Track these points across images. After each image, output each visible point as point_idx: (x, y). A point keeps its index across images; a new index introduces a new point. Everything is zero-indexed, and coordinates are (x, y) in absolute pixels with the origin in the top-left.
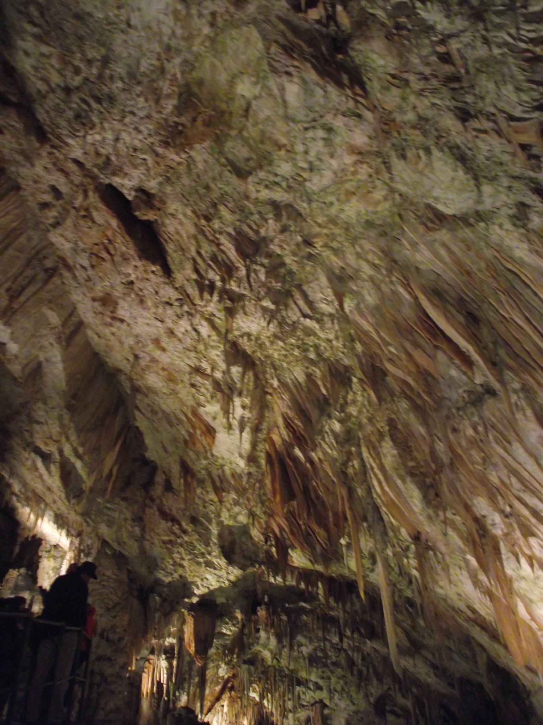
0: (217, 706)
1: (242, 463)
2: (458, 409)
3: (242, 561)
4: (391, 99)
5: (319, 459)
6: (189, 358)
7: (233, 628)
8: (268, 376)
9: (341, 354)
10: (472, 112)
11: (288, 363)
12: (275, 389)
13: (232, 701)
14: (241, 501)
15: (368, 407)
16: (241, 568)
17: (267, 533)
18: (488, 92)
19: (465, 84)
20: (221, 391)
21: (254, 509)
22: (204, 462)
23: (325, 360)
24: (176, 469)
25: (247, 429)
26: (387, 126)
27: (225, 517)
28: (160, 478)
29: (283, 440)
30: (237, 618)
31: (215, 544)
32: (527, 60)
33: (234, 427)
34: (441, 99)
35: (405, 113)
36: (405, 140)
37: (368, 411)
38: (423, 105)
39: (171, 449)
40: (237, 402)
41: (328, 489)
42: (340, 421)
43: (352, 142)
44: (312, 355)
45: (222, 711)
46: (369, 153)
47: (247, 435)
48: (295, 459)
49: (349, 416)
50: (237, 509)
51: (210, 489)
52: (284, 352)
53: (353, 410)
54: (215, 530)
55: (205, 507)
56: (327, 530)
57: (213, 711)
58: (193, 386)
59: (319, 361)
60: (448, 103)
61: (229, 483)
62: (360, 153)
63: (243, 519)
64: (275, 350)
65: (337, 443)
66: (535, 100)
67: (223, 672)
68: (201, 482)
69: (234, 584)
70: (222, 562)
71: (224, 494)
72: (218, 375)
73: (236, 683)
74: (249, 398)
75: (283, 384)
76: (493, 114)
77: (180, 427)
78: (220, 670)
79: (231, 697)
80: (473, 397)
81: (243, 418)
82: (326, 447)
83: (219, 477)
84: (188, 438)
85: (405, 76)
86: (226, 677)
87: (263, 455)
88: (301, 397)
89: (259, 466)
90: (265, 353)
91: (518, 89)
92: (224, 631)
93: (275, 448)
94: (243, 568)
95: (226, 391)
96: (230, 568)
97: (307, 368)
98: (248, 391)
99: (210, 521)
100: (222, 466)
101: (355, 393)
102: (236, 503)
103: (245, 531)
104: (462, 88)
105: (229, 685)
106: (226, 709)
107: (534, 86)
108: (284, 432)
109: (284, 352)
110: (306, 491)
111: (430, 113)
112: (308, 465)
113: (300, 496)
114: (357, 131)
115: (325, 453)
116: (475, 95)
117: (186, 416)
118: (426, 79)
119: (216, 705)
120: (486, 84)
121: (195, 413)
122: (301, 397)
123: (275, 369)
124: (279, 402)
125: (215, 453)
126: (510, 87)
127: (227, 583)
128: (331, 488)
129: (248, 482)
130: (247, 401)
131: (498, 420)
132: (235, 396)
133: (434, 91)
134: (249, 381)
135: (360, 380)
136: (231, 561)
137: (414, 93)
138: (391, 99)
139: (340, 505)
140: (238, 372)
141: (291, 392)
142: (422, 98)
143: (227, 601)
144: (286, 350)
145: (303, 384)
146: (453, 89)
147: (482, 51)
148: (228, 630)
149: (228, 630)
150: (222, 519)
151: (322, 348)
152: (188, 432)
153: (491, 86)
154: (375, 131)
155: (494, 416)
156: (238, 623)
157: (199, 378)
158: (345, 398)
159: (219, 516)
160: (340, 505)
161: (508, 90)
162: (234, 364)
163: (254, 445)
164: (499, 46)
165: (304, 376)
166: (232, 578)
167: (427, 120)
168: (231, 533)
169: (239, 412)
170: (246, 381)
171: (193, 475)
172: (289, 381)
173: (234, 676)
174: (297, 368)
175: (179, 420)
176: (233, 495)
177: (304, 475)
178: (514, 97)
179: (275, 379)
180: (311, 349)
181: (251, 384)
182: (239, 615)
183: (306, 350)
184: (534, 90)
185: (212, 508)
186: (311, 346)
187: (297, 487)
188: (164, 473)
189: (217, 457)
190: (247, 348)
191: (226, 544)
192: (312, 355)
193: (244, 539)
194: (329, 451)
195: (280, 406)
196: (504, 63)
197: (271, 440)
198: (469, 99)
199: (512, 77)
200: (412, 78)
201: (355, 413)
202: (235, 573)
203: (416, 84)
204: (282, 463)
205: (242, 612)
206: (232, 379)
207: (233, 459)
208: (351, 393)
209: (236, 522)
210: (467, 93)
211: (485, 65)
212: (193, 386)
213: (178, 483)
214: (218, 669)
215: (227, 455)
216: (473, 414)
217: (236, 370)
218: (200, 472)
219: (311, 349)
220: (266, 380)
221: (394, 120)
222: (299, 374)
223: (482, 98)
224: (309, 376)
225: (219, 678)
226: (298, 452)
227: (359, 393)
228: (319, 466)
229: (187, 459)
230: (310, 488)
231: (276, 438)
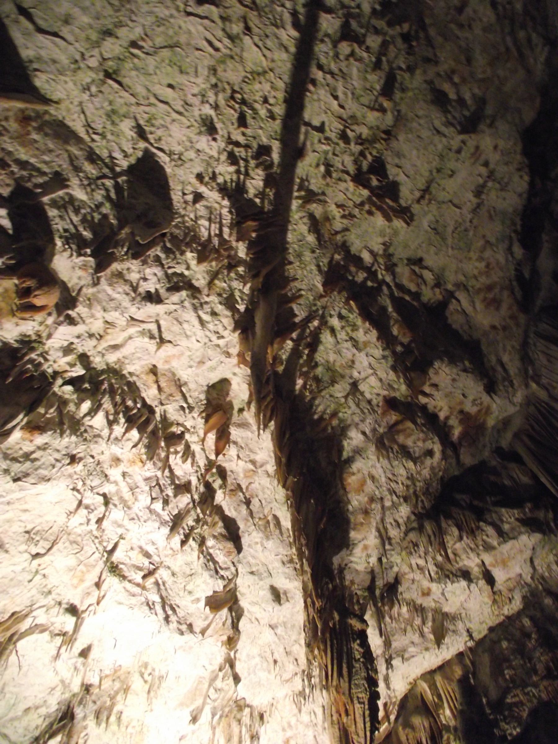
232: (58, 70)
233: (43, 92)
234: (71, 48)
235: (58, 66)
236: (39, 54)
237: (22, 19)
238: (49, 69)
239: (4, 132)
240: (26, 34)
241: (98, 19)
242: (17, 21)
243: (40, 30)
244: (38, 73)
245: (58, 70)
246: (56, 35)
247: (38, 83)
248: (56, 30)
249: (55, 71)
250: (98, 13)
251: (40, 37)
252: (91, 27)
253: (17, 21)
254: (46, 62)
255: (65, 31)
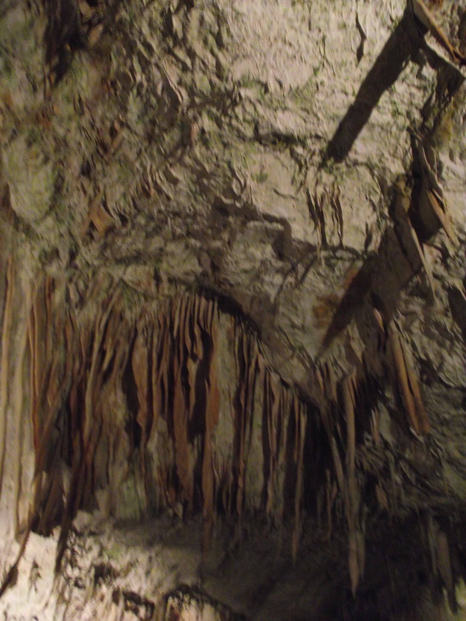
4: (64, 109)
10: (92, 175)
18: (110, 177)
19: (105, 157)
26: (43, 116)
32: (143, 188)
34: (86, 147)
35: (60, 125)
36: (42, 137)
38: (74, 137)
43: (12, 95)
46: (13, 114)
60: (87, 154)
62: (8, 107)
66: (124, 211)
76: (99, 190)
85: (86, 109)
91: (124, 195)
104: (102, 157)
107: (132, 204)
111: (72, 144)
114: (23, 93)
116: (103, 169)
118: (93, 126)
120: (114, 172)
126: (122, 189)
133: (89, 138)
137: (79, 123)
138: (64, 109)
142: (79, 131)
146: (98, 152)
147: (132, 156)
153: (115, 176)
154: (33, 109)
161: (120, 189)
164: (142, 165)
167: (66, 145)
178: (118, 196)
184: (129, 205)
196: (134, 174)
198: (99, 167)
199: (129, 186)
200: (87, 115)
203: (85, 122)
210: (102, 163)
211: (125, 162)
221: (49, 120)
223: (105, 175)
232: (381, 6)
233: (404, 6)
234: (359, 11)
235: (378, 9)
236: (380, 27)
237: (365, 51)
238: (385, 14)
239: (456, 7)
240: (373, 44)
241: (326, 9)
242: (369, 54)
243: (363, 37)
244: (394, 18)
245: (381, 6)
246: (358, 26)
247: (401, 13)
248: (355, 29)
249: (383, 8)
250: (322, 12)
251: (368, 34)
252: (335, 8)
253: (369, 54)
254: (382, 19)
255: (351, 22)
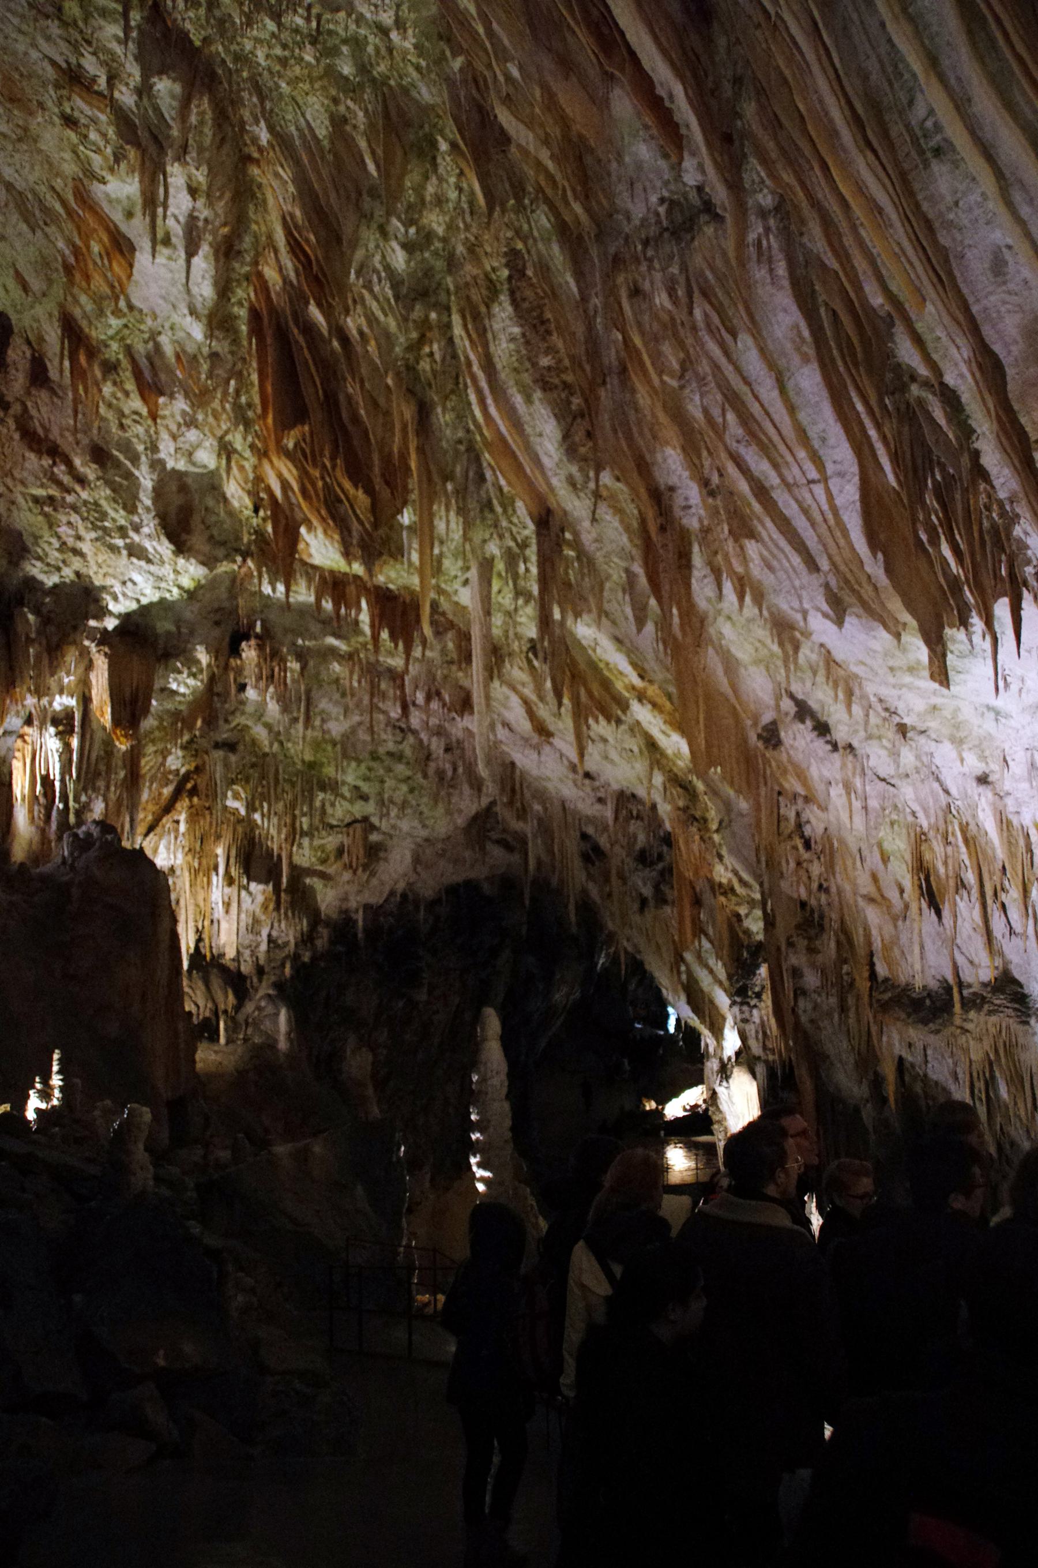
0: (167, 821)
1: (197, 331)
2: (646, 243)
3: (206, 548)
5: (361, 333)
6: (48, 38)
7: (191, 682)
8: (247, 115)
9: (415, 74)
11: (294, 82)
12: (260, 150)
13: (194, 817)
14: (200, 417)
15: (468, 219)
16: (203, 563)
17: (257, 487)
20: (137, 144)
21: (229, 438)
22: (115, 322)
23: (379, 84)
24: (53, 335)
25: (205, 249)
27: (166, 449)
28: (17, 354)
29: (285, 280)
30: (198, 662)
31: (148, 509)
33: (174, 240)
37: (467, 228)
39: (36, 284)
40: (177, 176)
41: (375, 404)
42: (408, 247)
44: (347, 69)
45: (177, 830)
47: (202, 263)
48: (308, 328)
49: (429, 236)
50: (192, 435)
51: (130, 386)
52: (278, 51)
53: (436, 221)
54: (146, 480)
55: (122, 426)
56: (370, 491)
57: (158, 830)
58: (70, 121)
59: (361, 86)
61: (171, 372)
63: (207, 458)
64: (258, 40)
65: (397, 297)
67: (176, 761)
68: (110, 368)
69: (191, 595)
70: (164, 548)
71: (162, 400)
72: (126, 97)
73: (202, 781)
74: (204, 169)
75: (281, 139)
77: (51, 230)
78: (170, 760)
79: (191, 807)
80: (679, 218)
81: (192, 218)
82: (374, 305)
83: (149, 358)
84: (72, 260)
86: (183, 771)
87: (243, 313)
88: (320, 178)
89: (236, 341)
90: (234, 47)
92: (174, 686)
93: (268, 298)
94: (208, 562)
95: (147, 144)
96: (181, 561)
97: (335, 101)
98: (201, 150)
99: (135, 459)
100: (154, 335)
101: (441, 179)
102: (191, 422)
103: (212, 484)
105: (189, 786)
106: (182, 827)
108: (288, 263)
109: (278, 51)
110: (331, 402)
112: (335, 344)
113: (317, 415)
115: (371, 319)
117: (64, 203)
119: (164, 820)
121: (83, 197)
122: (320, 178)
123: (262, 99)
124: (275, 184)
125: (136, 302)
127: (175, 591)
128: (382, 401)
129: (210, 375)
130: (200, 176)
131: (718, 279)
132: (168, 159)
134: (202, 123)
135: (454, 145)
136: (181, 549)
139: (397, 439)
140: (173, 97)
141: (297, 162)
143: (178, 628)
144: (285, 47)
145: (326, 143)
148: (184, 684)
149: (184, 684)
150: (162, 455)
151: (370, 49)
152: (70, 242)
155: (712, 268)
156: (201, 671)
157: (79, 102)
158: (419, 189)
159: (154, 448)
160: (397, 439)
162: (161, 72)
163: (224, 289)
165: (327, 123)
166: (187, 582)
168: (183, 488)
169: (180, 203)
170: (193, 119)
171: (92, 353)
172: (295, 133)
173: (198, 770)
174: (311, 99)
175: (46, 210)
176: (181, 404)
177: (328, 368)
179: (262, 124)
180: (345, 49)
181: (208, 131)
182: (203, 656)
183: (333, 52)
185: (140, 430)
186: (345, 41)
187: (312, 393)
188: (29, 343)
189: (141, 311)
190: (188, 26)
191: (173, 510)
192: (347, 69)
193: (210, 502)
194: (379, 314)
195: (277, 190)
197: (260, 275)
201: (440, 231)
202: (191, 572)
204: (282, 335)
205: (208, 652)
206: (157, 109)
207: (176, 318)
208: (434, 180)
209: (194, 464)
212: (70, 121)
213: (59, 369)
214: (165, 758)
215: (163, 308)
216: (671, 257)
217: (164, 86)
218: (107, 346)
219: (345, 49)
220: (242, 123)
222: (314, 113)
224: (339, 123)
225: (170, 772)
226: (315, 312)
227: (452, 180)
228: (359, 349)
229: (77, 312)
230: (342, 397)
231: (270, 273)
